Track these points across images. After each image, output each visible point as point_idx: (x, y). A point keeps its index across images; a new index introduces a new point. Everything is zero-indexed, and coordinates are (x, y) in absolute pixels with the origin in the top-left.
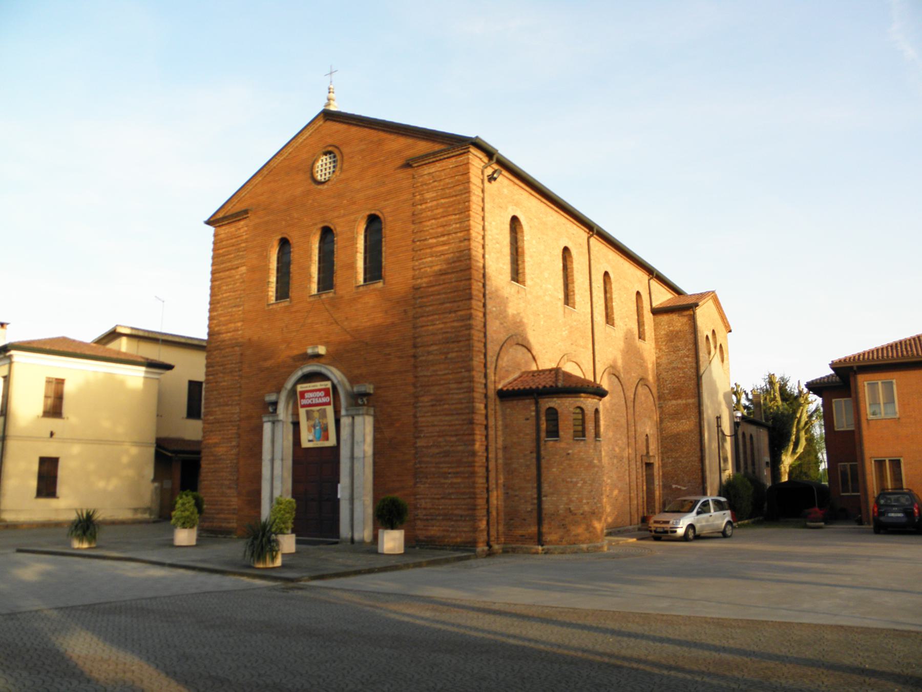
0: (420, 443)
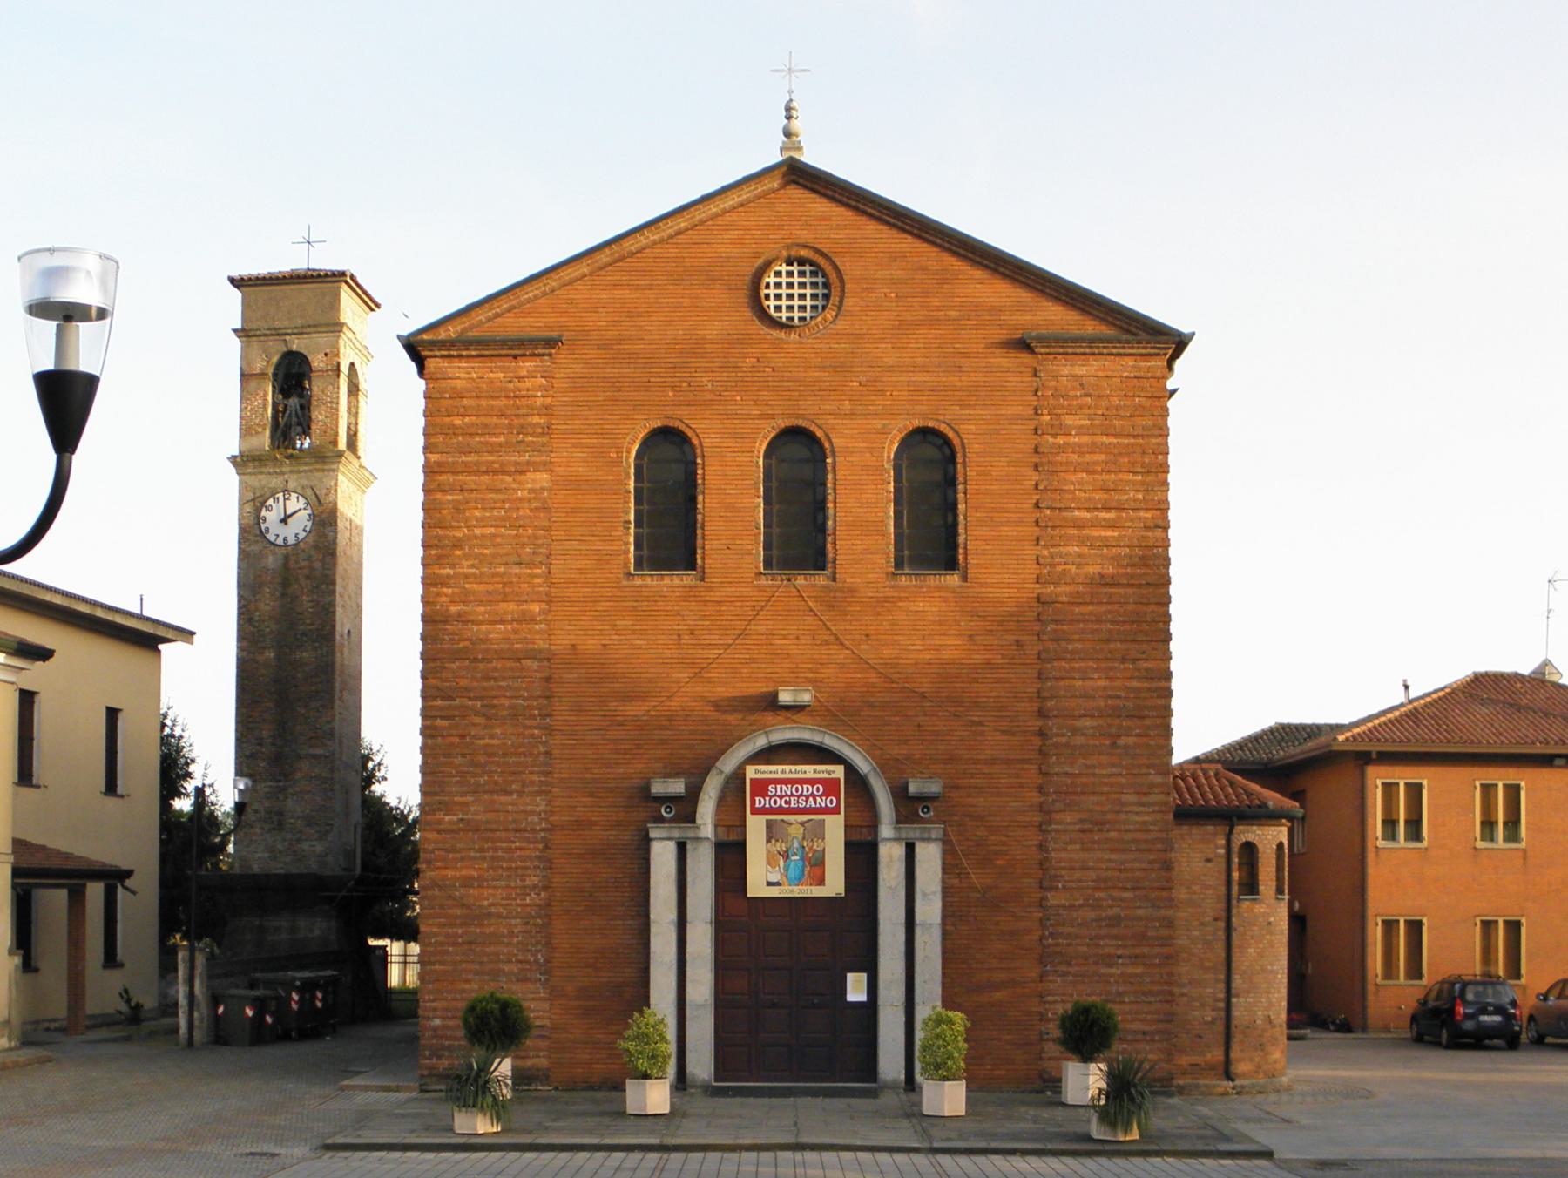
0: (1053, 900)
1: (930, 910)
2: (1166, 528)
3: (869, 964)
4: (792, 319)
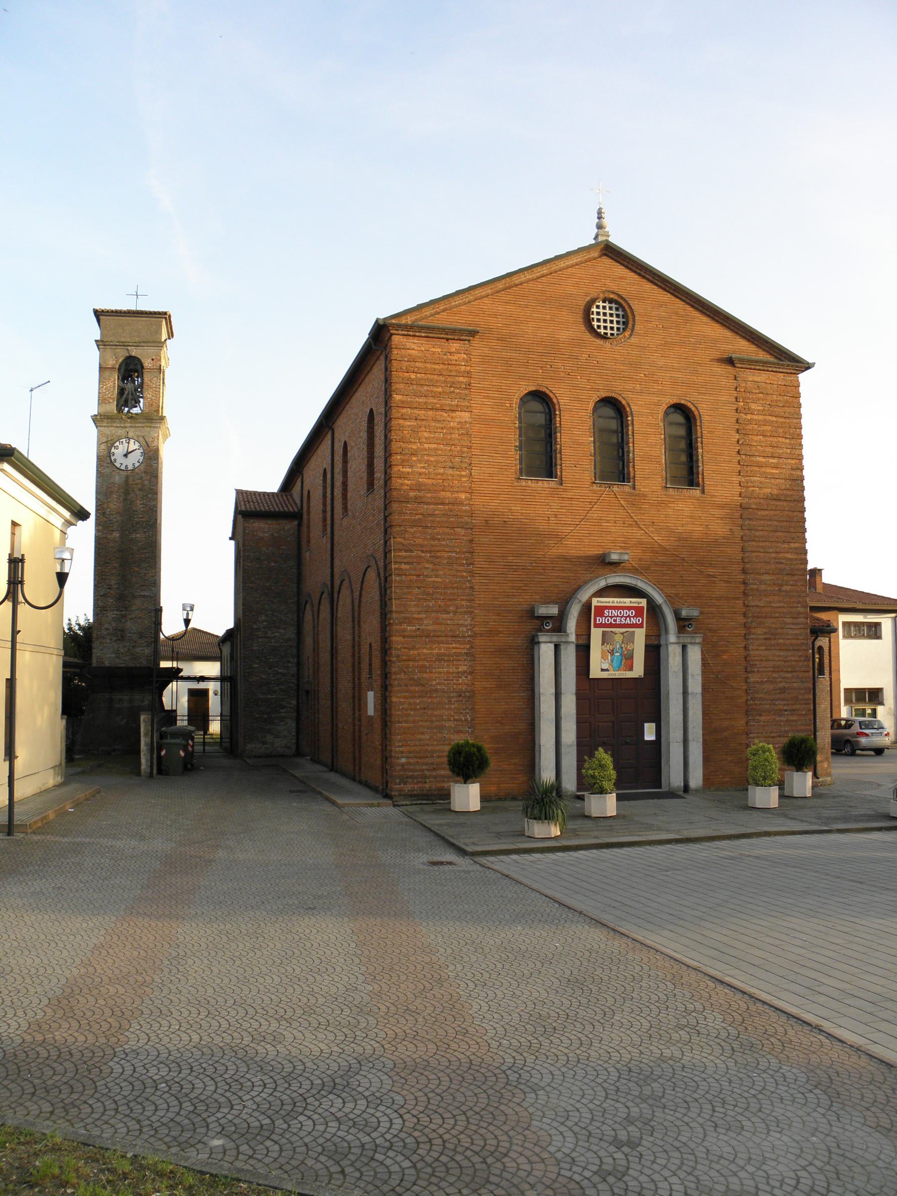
0: (753, 678)
1: (696, 685)
2: (802, 469)
3: (657, 718)
4: (606, 334)
